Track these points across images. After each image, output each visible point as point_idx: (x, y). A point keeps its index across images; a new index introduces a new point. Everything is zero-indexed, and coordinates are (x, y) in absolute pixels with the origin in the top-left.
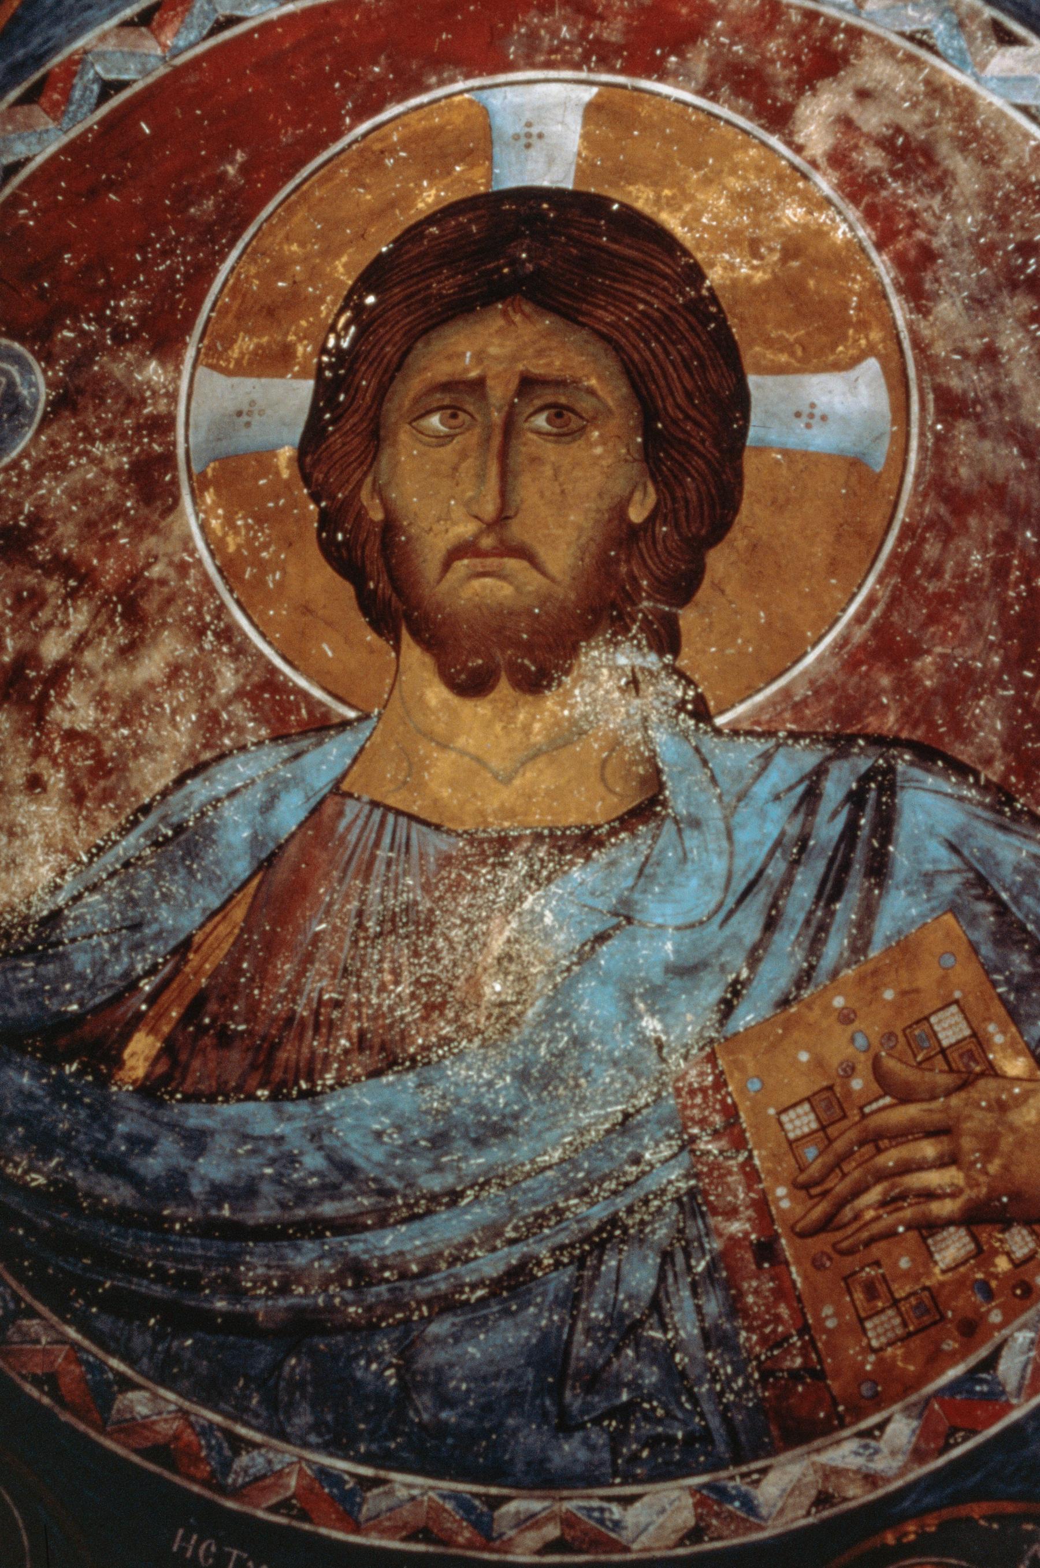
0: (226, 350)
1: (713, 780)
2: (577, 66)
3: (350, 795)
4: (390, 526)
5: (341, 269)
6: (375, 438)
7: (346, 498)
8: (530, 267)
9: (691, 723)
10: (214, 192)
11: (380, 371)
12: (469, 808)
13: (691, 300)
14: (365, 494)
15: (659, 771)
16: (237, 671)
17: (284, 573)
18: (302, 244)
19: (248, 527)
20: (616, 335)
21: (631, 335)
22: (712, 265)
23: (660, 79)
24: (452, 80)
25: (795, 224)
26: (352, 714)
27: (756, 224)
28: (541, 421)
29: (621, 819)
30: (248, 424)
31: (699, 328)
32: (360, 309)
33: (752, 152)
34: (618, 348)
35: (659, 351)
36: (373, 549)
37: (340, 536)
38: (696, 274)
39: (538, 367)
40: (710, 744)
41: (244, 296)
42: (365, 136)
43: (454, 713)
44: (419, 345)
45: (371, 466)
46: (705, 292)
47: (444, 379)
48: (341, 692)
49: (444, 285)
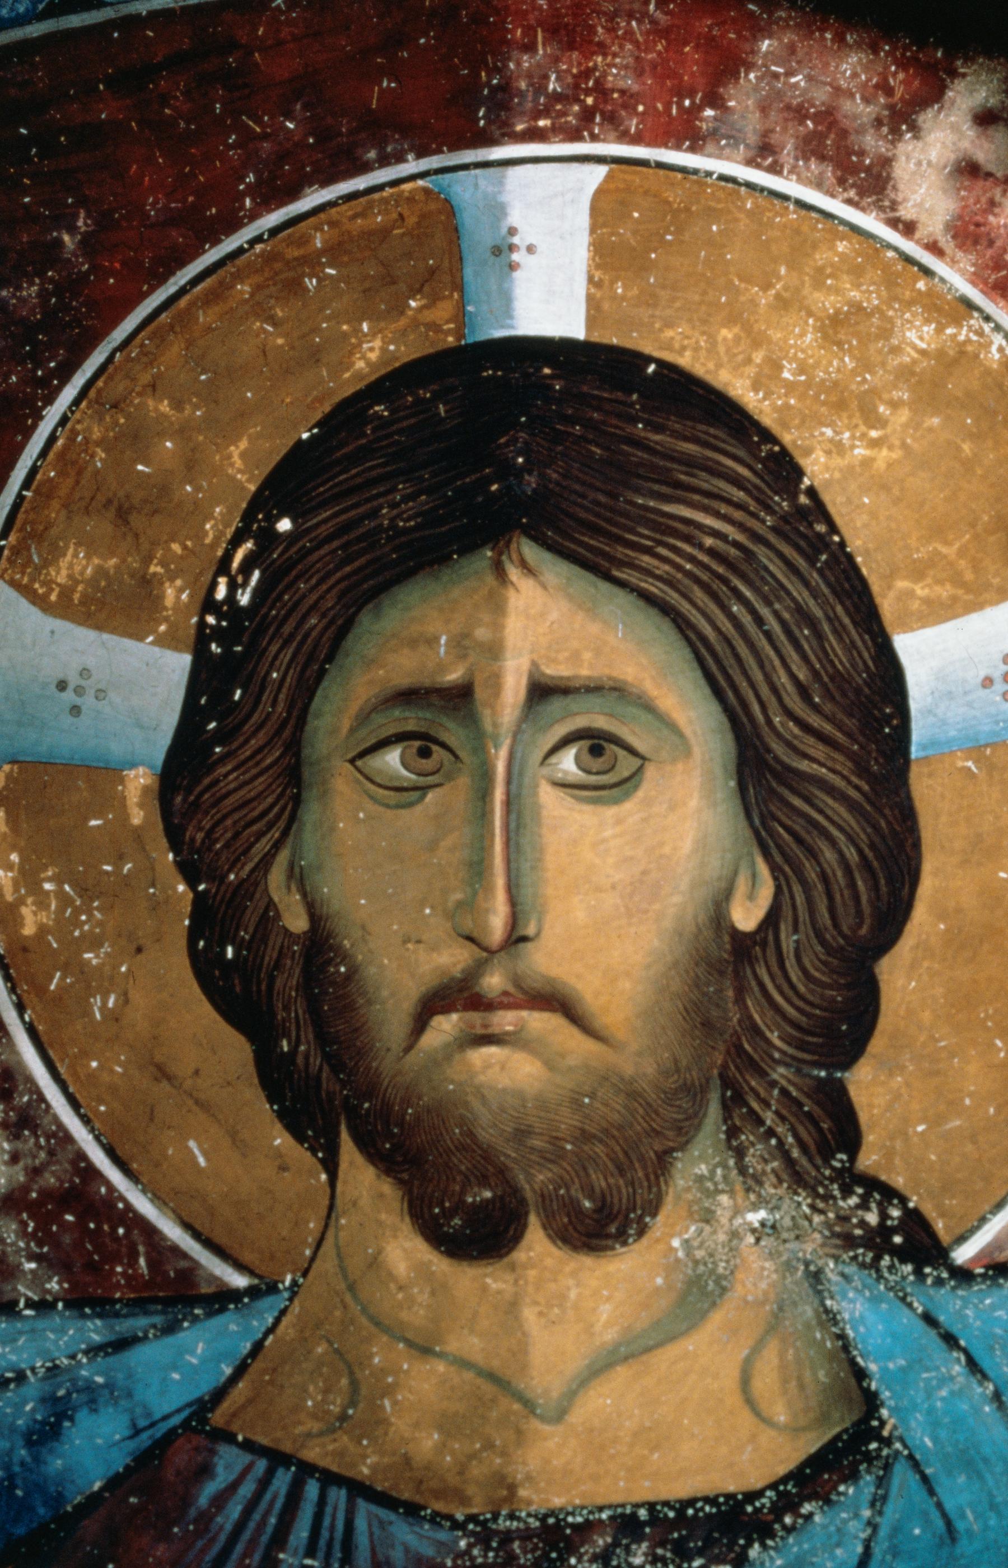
0: (46, 564)
1: (973, 1365)
2: (575, 136)
3: (229, 1438)
4: (320, 944)
5: (239, 463)
6: (293, 780)
7: (241, 883)
8: (531, 481)
9: (908, 1268)
10: (41, 274)
11: (301, 659)
12: (476, 1471)
13: (784, 518)
14: (276, 877)
15: (860, 1374)
16: (15, 1158)
17: (125, 999)
18: (178, 405)
19: (65, 900)
20: (673, 597)
21: (698, 594)
22: (808, 452)
23: (693, 149)
24: (400, 159)
25: (923, 353)
26: (240, 1281)
27: (865, 365)
28: (567, 762)
29: (796, 1475)
30: (75, 710)
31: (801, 563)
32: (268, 537)
33: (841, 246)
34: (681, 624)
35: (747, 619)
36: (289, 981)
37: (230, 952)
38: (784, 469)
39: (556, 670)
40: (953, 1305)
41: (80, 473)
42: (274, 231)
43: (439, 1288)
44: (365, 619)
45: (285, 833)
46: (803, 499)
47: (403, 681)
48: (220, 1238)
49: (399, 509)
